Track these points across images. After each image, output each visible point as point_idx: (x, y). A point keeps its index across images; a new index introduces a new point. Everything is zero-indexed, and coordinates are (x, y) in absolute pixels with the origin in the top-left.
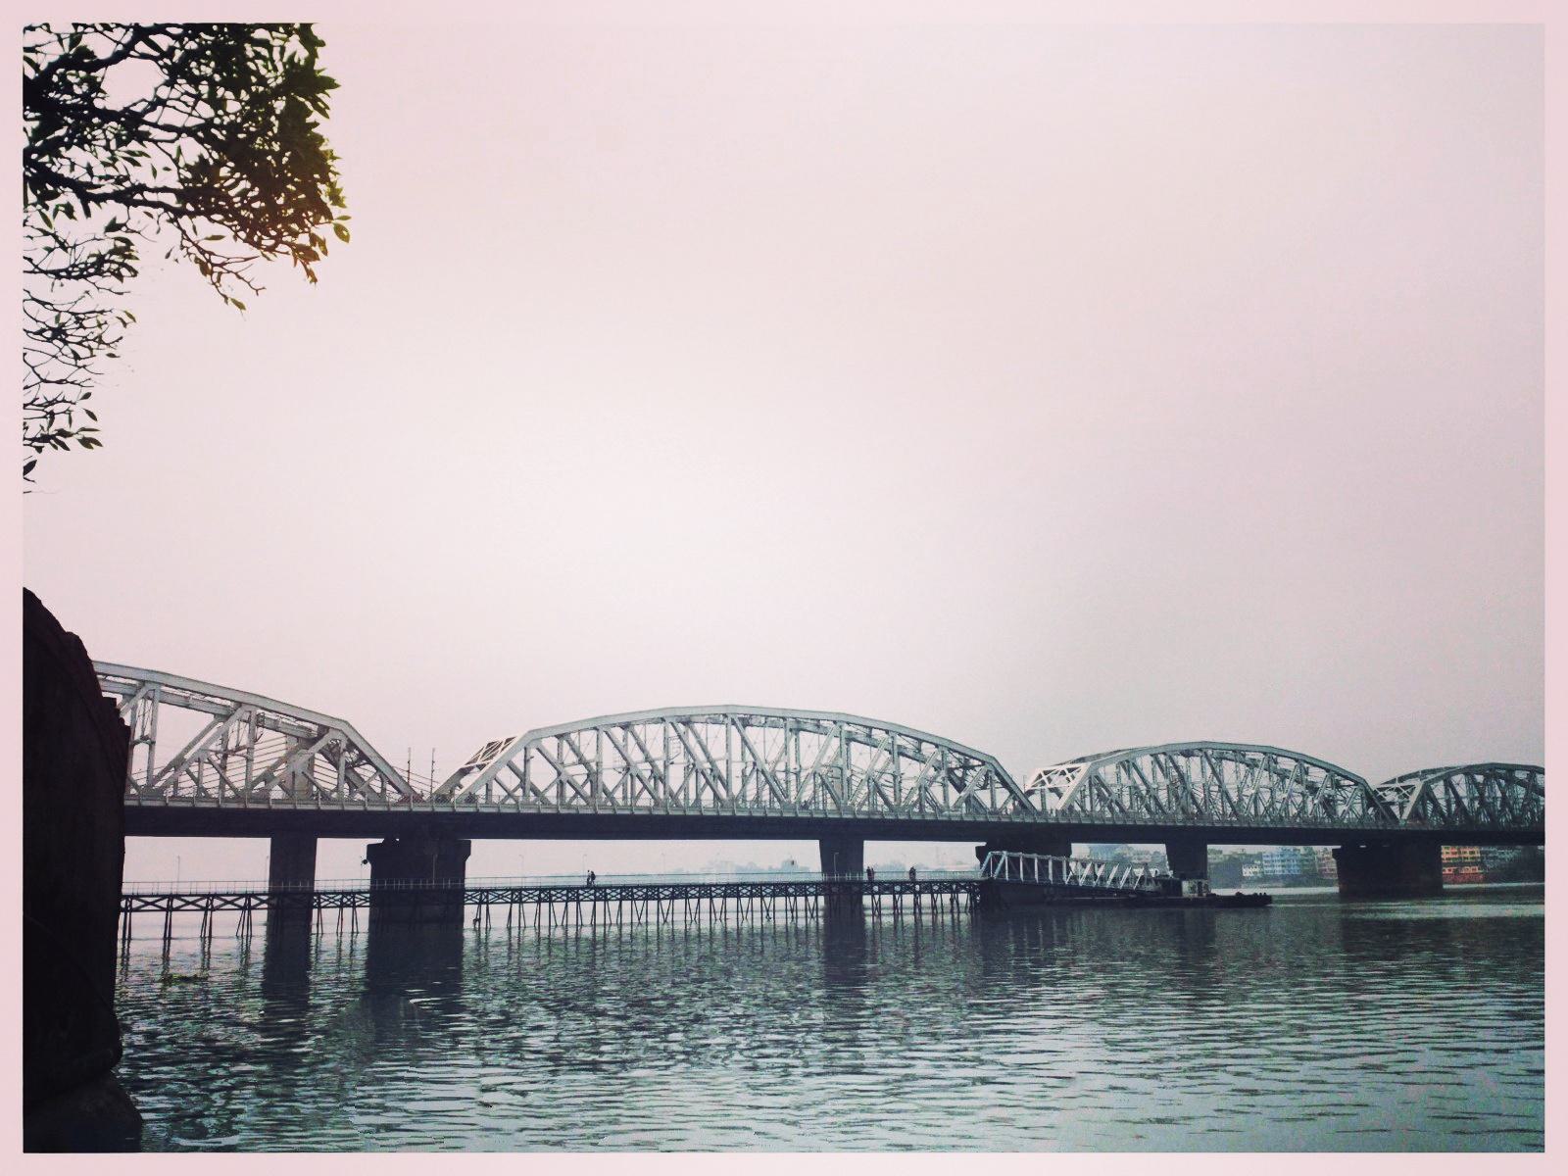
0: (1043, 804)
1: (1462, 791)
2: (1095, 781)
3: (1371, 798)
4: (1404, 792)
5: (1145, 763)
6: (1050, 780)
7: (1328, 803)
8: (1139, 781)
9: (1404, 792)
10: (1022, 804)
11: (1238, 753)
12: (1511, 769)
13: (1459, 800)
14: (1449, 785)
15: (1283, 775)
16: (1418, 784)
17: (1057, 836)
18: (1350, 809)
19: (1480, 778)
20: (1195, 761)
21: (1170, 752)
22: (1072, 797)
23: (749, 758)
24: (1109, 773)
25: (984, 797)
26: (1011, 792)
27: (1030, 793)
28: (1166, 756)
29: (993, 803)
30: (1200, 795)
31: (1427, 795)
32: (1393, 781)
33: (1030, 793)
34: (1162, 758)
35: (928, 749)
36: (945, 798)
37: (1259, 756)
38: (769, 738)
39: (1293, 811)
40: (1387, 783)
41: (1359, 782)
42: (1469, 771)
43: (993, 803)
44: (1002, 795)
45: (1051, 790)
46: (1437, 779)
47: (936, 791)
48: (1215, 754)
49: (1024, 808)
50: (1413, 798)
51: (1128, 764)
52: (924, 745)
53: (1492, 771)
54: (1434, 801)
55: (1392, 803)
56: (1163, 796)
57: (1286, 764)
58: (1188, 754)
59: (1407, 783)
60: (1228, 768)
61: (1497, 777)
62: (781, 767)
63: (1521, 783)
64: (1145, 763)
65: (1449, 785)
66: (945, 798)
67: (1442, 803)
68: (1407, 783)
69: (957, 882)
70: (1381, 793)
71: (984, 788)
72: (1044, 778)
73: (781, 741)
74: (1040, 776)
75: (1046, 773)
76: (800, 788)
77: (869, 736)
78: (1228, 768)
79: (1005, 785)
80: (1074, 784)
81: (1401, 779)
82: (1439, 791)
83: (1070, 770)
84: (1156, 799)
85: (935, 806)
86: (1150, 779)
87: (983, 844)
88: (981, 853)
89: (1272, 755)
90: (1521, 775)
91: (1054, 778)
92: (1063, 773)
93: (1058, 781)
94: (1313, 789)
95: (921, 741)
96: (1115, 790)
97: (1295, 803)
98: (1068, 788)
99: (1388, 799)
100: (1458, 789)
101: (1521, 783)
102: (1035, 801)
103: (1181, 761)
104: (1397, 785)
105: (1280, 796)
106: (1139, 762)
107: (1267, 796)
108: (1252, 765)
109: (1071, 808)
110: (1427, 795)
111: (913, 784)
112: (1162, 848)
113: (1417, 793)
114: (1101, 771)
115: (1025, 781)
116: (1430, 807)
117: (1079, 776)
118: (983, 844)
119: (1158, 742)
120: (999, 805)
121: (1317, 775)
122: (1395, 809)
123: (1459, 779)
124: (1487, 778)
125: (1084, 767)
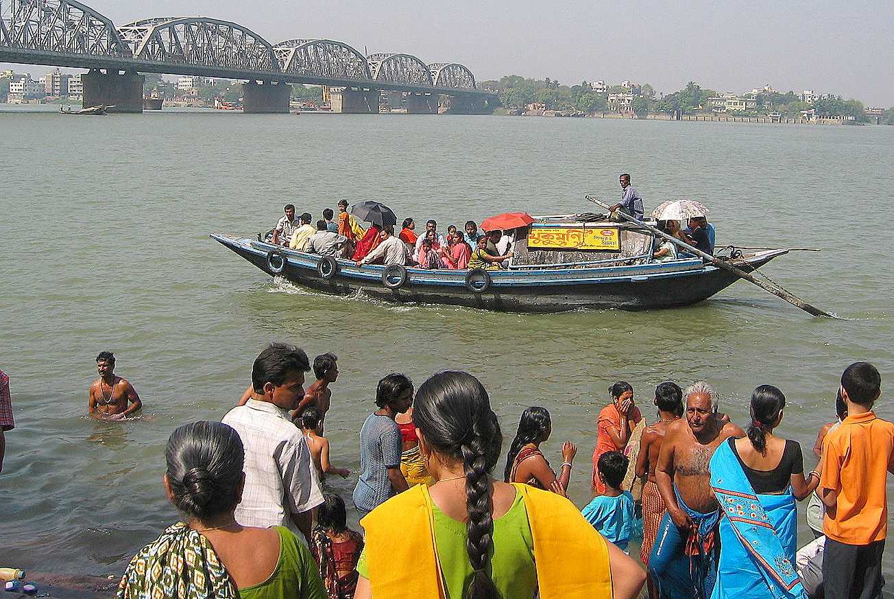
1: (181, 37)
3: (115, 36)
4: (139, 33)
7: (81, 38)
9: (140, 33)
12: (218, 23)
13: (178, 43)
14: (173, 33)
16: (150, 29)
40: (127, 26)
41: (107, 24)
42: (188, 23)
46: (163, 27)
50: (145, 39)
53: (204, 23)
55: (130, 42)
61: (206, 29)
63: (221, 34)
65: (173, 33)
67: (166, 46)
70: (122, 33)
82: (165, 35)
90: (223, 28)
94: (71, 24)
99: (127, 39)
101: (221, 34)
104: (136, 28)
105: (45, 29)
110: (156, 37)
113: (150, 32)
122: (132, 46)
123: (180, 28)
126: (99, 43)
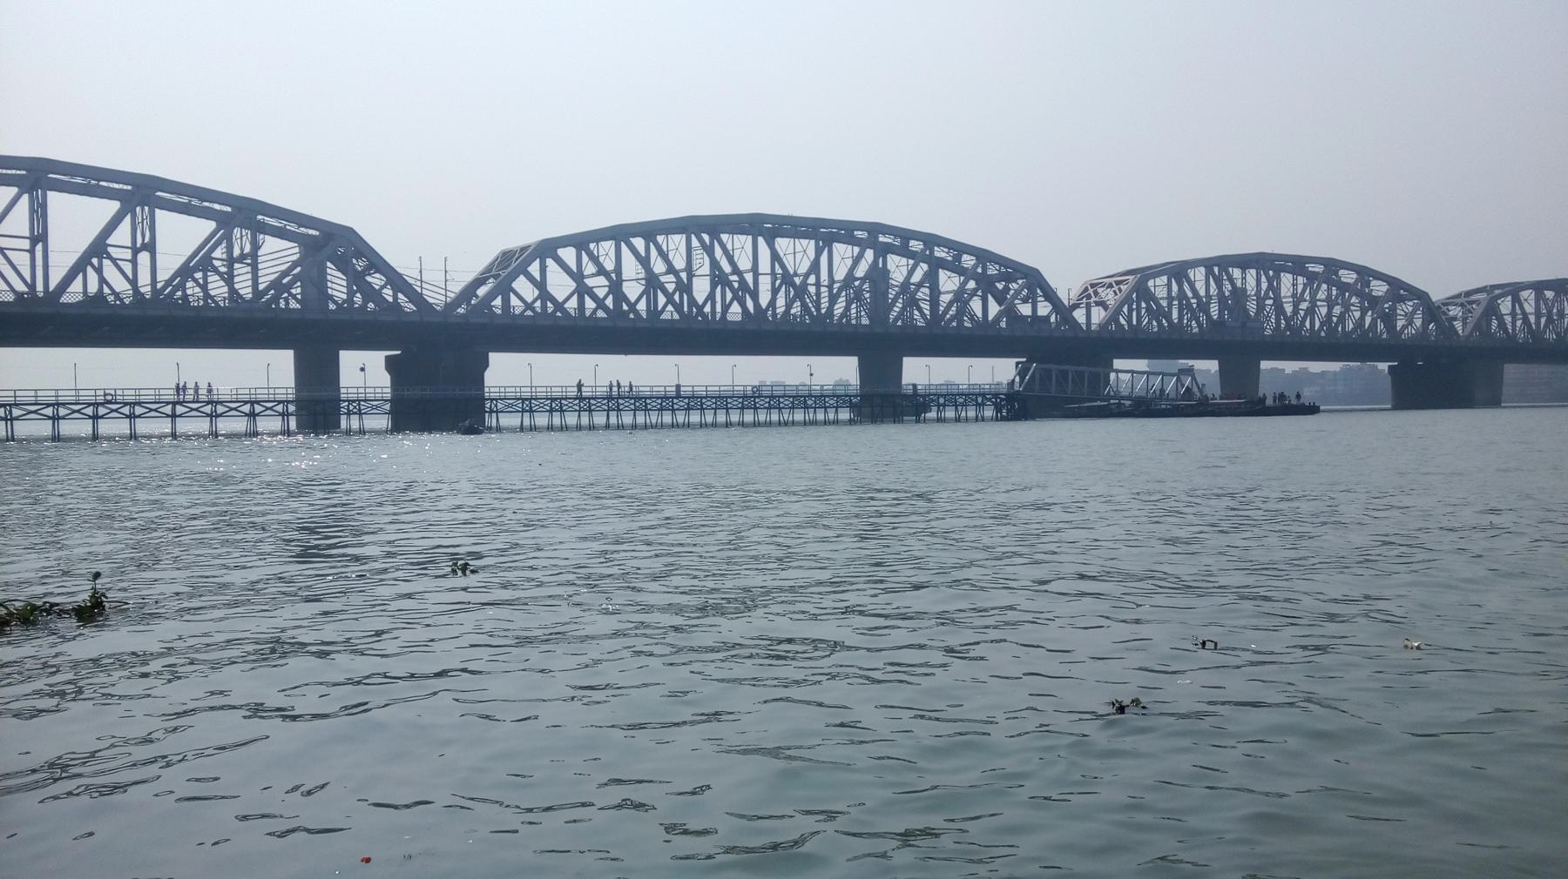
1: (1529, 308)
3: (1432, 311)
5: (1198, 275)
6: (1096, 293)
7: (1389, 319)
11: (1297, 264)
13: (1525, 315)
14: (1516, 300)
15: (1343, 287)
18: (1409, 322)
19: (1549, 294)
20: (1252, 274)
21: (1225, 262)
22: (1118, 311)
23: (779, 270)
24: (1158, 286)
25: (1025, 310)
27: (1076, 306)
28: (1218, 266)
31: (1492, 310)
32: (1459, 296)
34: (1216, 269)
37: (1319, 269)
38: (799, 248)
41: (1422, 296)
42: (1539, 287)
44: (1044, 309)
47: (976, 305)
54: (1500, 318)
55: (1455, 319)
56: (1214, 310)
57: (1348, 277)
59: (1474, 297)
60: (1286, 279)
62: (812, 280)
65: (1516, 300)
67: (1508, 319)
68: (1474, 297)
71: (1025, 301)
72: (1091, 291)
73: (812, 254)
74: (1086, 289)
75: (1093, 286)
76: (833, 299)
78: (1286, 279)
81: (1468, 294)
82: (1505, 306)
83: (1118, 283)
85: (972, 317)
86: (1202, 293)
89: (1333, 266)
92: (1110, 286)
94: (1374, 302)
96: (1164, 303)
97: (1355, 316)
100: (1526, 306)
102: (1079, 315)
103: (1237, 273)
105: (1337, 310)
107: (1324, 311)
108: (1312, 278)
112: (1212, 366)
116: (1495, 323)
121: (1379, 289)
122: (1458, 325)
124: (1557, 295)
126: (1410, 323)
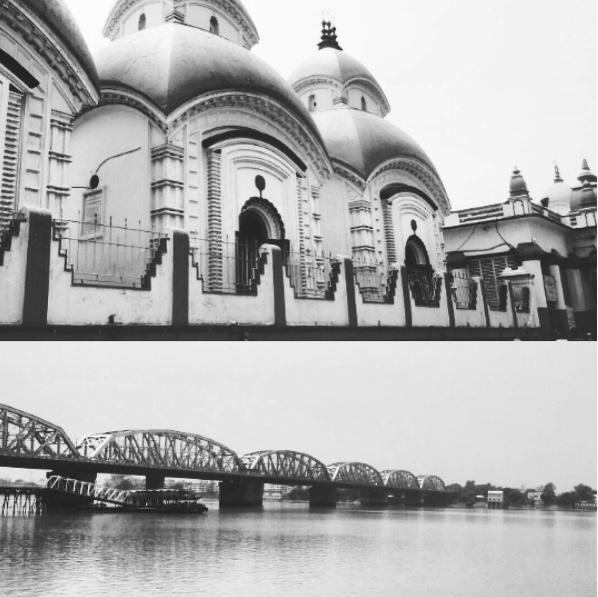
0: (85, 453)
2: (113, 444)
5: (139, 437)
8: (135, 445)
10: (74, 452)
11: (183, 437)
16: (258, 457)
17: (88, 470)
20: (163, 439)
22: (100, 451)
24: (120, 441)
25: (54, 448)
26: (69, 446)
27: (80, 447)
28: (148, 435)
29: (58, 451)
30: (163, 454)
33: (80, 447)
35: (25, 421)
36: (32, 447)
37: (192, 439)
39: (204, 465)
43: (58, 451)
44: (64, 448)
45: (91, 447)
47: (27, 443)
48: (173, 436)
49: (75, 453)
51: (130, 437)
52: (23, 419)
56: (146, 454)
57: (204, 444)
58: (160, 435)
64: (139, 437)
66: (32, 447)
69: (30, 489)
77: (20, 421)
79: (66, 442)
80: (102, 444)
84: (142, 455)
86: (140, 445)
87: (50, 471)
88: (48, 475)
89: (198, 439)
91: (93, 440)
93: (94, 443)
94: (214, 455)
95: (21, 416)
96: (122, 449)
98: (100, 446)
102: (81, 452)
103: (156, 438)
106: (136, 436)
109: (99, 456)
110: (260, 462)
111: (14, 438)
112: (143, 477)
114: (117, 440)
115: (77, 441)
117: (105, 441)
118: (50, 471)
119: (146, 428)
120: (61, 452)
121: (216, 449)
125: (109, 437)
